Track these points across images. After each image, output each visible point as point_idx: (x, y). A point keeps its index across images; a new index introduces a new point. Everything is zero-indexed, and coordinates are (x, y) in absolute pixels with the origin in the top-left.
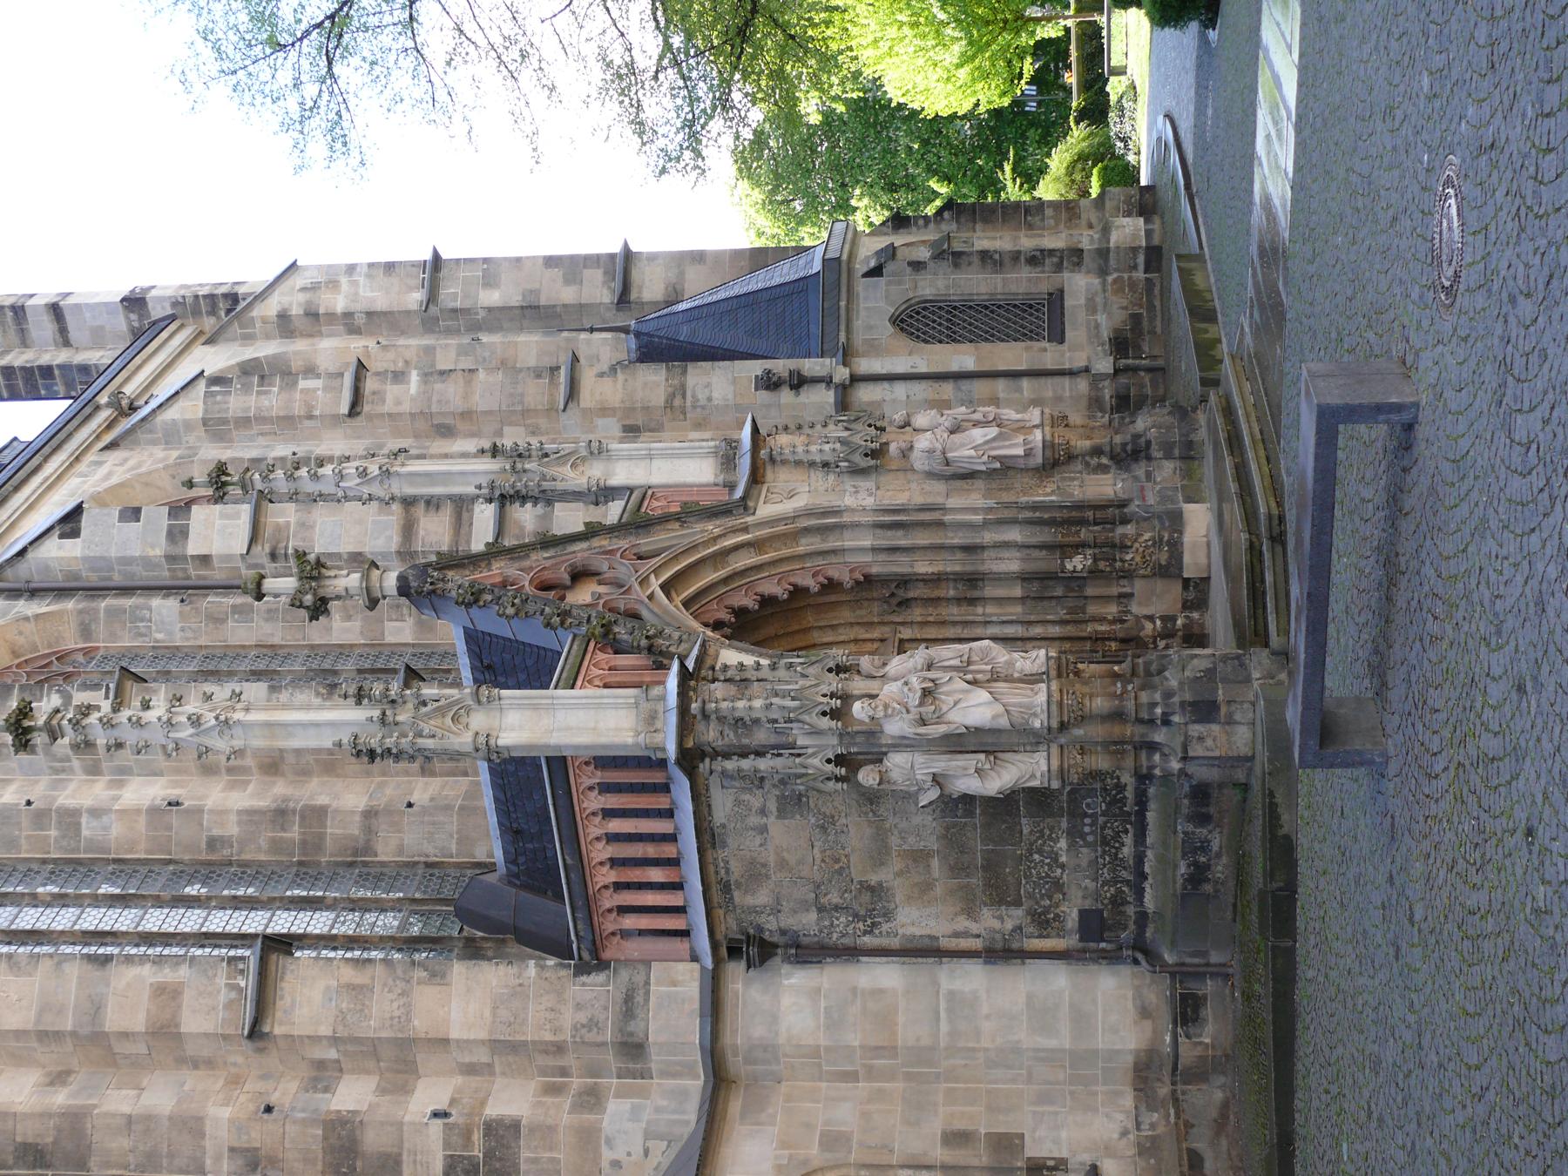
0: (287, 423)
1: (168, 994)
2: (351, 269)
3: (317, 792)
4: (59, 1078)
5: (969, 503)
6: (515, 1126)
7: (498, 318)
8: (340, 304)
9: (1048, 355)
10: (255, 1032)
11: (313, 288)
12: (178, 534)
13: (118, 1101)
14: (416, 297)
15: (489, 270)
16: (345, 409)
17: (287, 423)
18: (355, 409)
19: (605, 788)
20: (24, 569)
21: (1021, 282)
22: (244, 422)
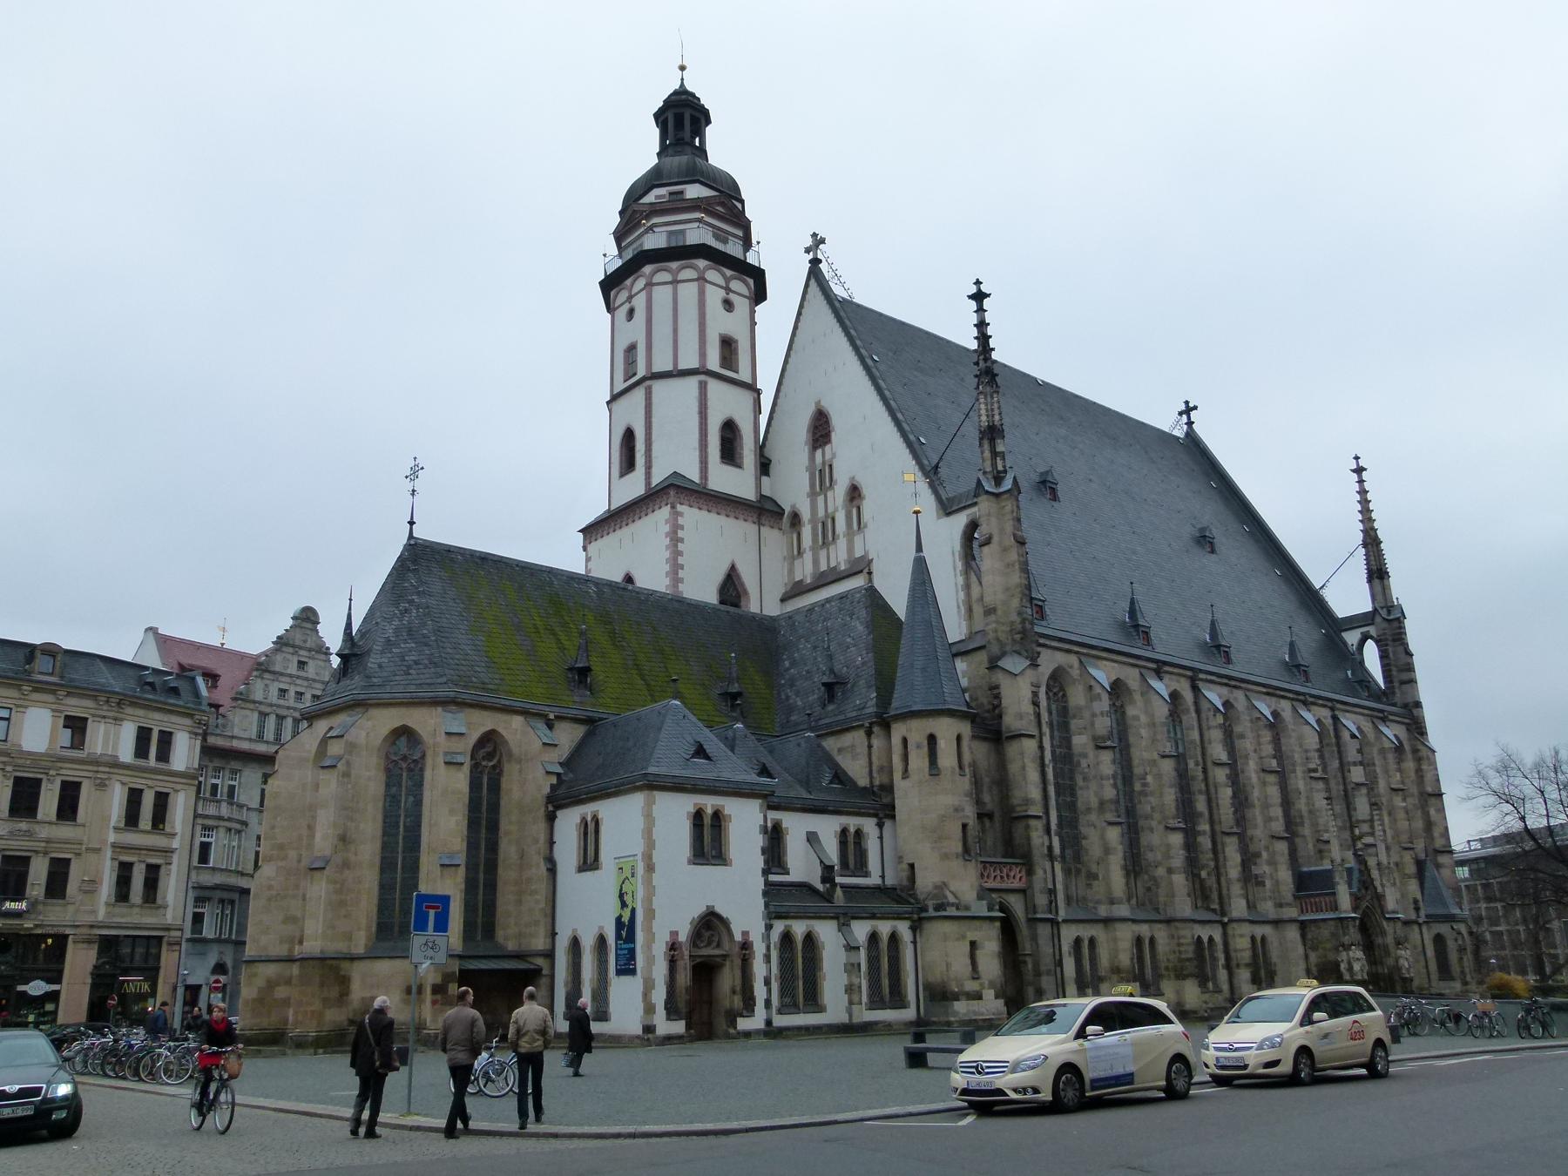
0: (1386, 771)
1: (1277, 819)
2: (1436, 769)
3: (1307, 823)
4: (1259, 800)
5: (1390, 961)
6: (1264, 886)
7: (1426, 815)
8: (1424, 767)
9: (1435, 976)
10: (1273, 837)
11: (1428, 758)
12: (1355, 764)
13: (1257, 812)
14: (1429, 789)
15: (1442, 810)
16: (1393, 786)
17: (1386, 771)
18: (1393, 789)
19: (1330, 902)
20: (1340, 725)
21: (1455, 968)
22: (1385, 758)
